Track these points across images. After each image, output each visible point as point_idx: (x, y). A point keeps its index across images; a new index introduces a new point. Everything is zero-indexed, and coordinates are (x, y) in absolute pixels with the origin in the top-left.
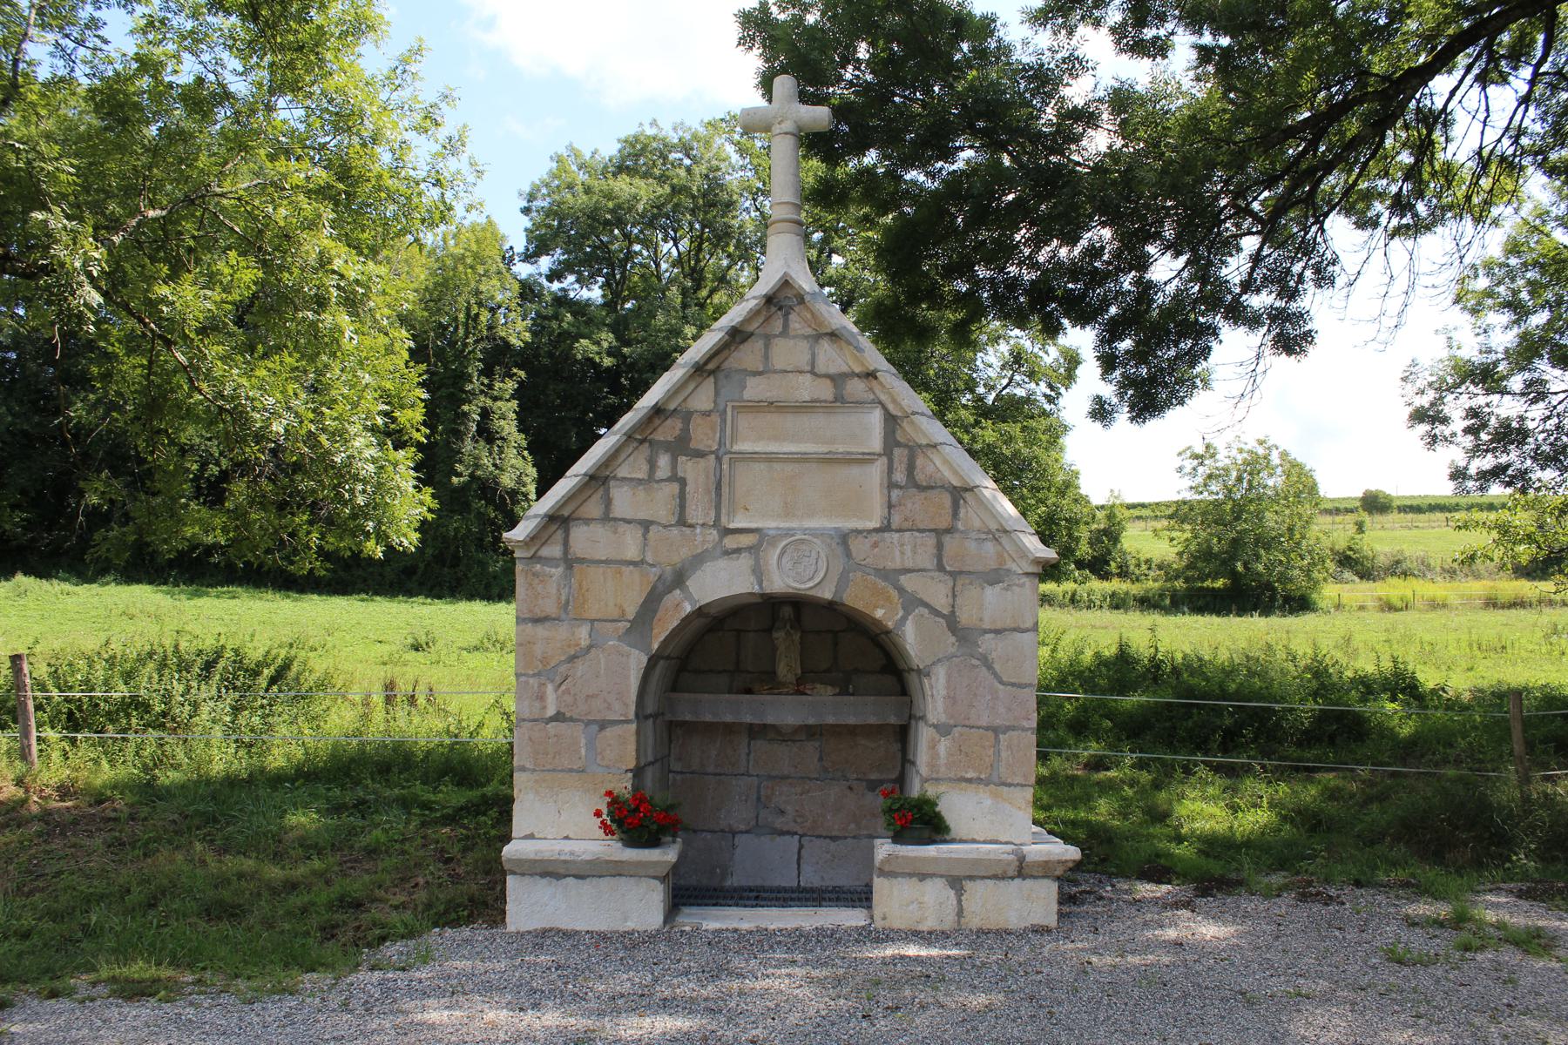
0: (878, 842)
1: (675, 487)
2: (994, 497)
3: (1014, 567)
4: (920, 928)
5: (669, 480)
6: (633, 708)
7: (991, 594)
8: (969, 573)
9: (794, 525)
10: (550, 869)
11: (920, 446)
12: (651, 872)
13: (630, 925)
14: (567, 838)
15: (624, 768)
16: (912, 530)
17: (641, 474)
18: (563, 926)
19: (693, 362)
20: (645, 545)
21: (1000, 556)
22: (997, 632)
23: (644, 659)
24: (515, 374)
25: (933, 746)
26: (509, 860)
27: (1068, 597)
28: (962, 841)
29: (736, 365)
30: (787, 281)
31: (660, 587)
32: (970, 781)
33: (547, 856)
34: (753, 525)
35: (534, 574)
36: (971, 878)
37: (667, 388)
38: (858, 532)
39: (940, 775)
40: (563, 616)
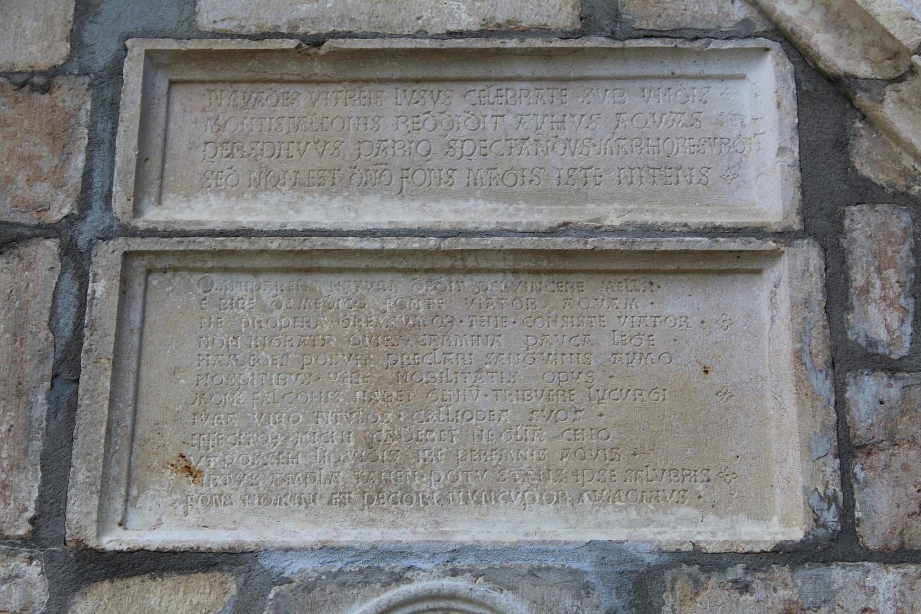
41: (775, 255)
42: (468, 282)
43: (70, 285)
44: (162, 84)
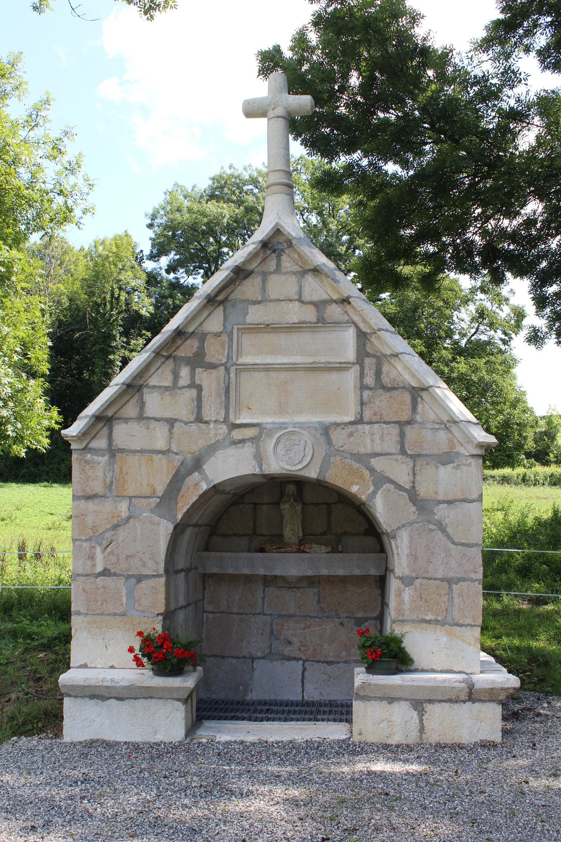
0: (357, 670)
1: (193, 393)
2: (446, 396)
3: (462, 450)
4: (390, 742)
5: (189, 386)
6: (162, 565)
7: (444, 472)
8: (426, 455)
9: (286, 420)
10: (97, 693)
11: (385, 356)
12: (175, 695)
13: (159, 738)
14: (112, 667)
15: (156, 612)
16: (381, 422)
17: (168, 383)
18: (107, 738)
19: (206, 294)
20: (171, 438)
21: (451, 441)
22: (449, 502)
23: (171, 527)
24: (144, 334)
25: (399, 594)
26: (64, 686)
27: (520, 478)
28: (423, 671)
29: (240, 297)
30: (278, 229)
31: (183, 471)
32: (429, 622)
33: (93, 683)
34: (255, 421)
35: (86, 462)
36: (430, 701)
37: (186, 315)
38: (337, 425)
39: (405, 618)
40: (108, 494)
41: (351, 367)
42: (297, 373)
43: (227, 375)
44: (240, 334)
